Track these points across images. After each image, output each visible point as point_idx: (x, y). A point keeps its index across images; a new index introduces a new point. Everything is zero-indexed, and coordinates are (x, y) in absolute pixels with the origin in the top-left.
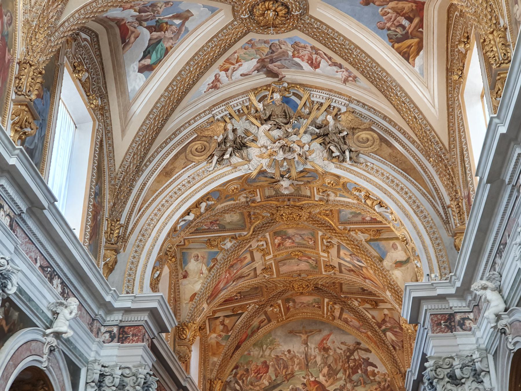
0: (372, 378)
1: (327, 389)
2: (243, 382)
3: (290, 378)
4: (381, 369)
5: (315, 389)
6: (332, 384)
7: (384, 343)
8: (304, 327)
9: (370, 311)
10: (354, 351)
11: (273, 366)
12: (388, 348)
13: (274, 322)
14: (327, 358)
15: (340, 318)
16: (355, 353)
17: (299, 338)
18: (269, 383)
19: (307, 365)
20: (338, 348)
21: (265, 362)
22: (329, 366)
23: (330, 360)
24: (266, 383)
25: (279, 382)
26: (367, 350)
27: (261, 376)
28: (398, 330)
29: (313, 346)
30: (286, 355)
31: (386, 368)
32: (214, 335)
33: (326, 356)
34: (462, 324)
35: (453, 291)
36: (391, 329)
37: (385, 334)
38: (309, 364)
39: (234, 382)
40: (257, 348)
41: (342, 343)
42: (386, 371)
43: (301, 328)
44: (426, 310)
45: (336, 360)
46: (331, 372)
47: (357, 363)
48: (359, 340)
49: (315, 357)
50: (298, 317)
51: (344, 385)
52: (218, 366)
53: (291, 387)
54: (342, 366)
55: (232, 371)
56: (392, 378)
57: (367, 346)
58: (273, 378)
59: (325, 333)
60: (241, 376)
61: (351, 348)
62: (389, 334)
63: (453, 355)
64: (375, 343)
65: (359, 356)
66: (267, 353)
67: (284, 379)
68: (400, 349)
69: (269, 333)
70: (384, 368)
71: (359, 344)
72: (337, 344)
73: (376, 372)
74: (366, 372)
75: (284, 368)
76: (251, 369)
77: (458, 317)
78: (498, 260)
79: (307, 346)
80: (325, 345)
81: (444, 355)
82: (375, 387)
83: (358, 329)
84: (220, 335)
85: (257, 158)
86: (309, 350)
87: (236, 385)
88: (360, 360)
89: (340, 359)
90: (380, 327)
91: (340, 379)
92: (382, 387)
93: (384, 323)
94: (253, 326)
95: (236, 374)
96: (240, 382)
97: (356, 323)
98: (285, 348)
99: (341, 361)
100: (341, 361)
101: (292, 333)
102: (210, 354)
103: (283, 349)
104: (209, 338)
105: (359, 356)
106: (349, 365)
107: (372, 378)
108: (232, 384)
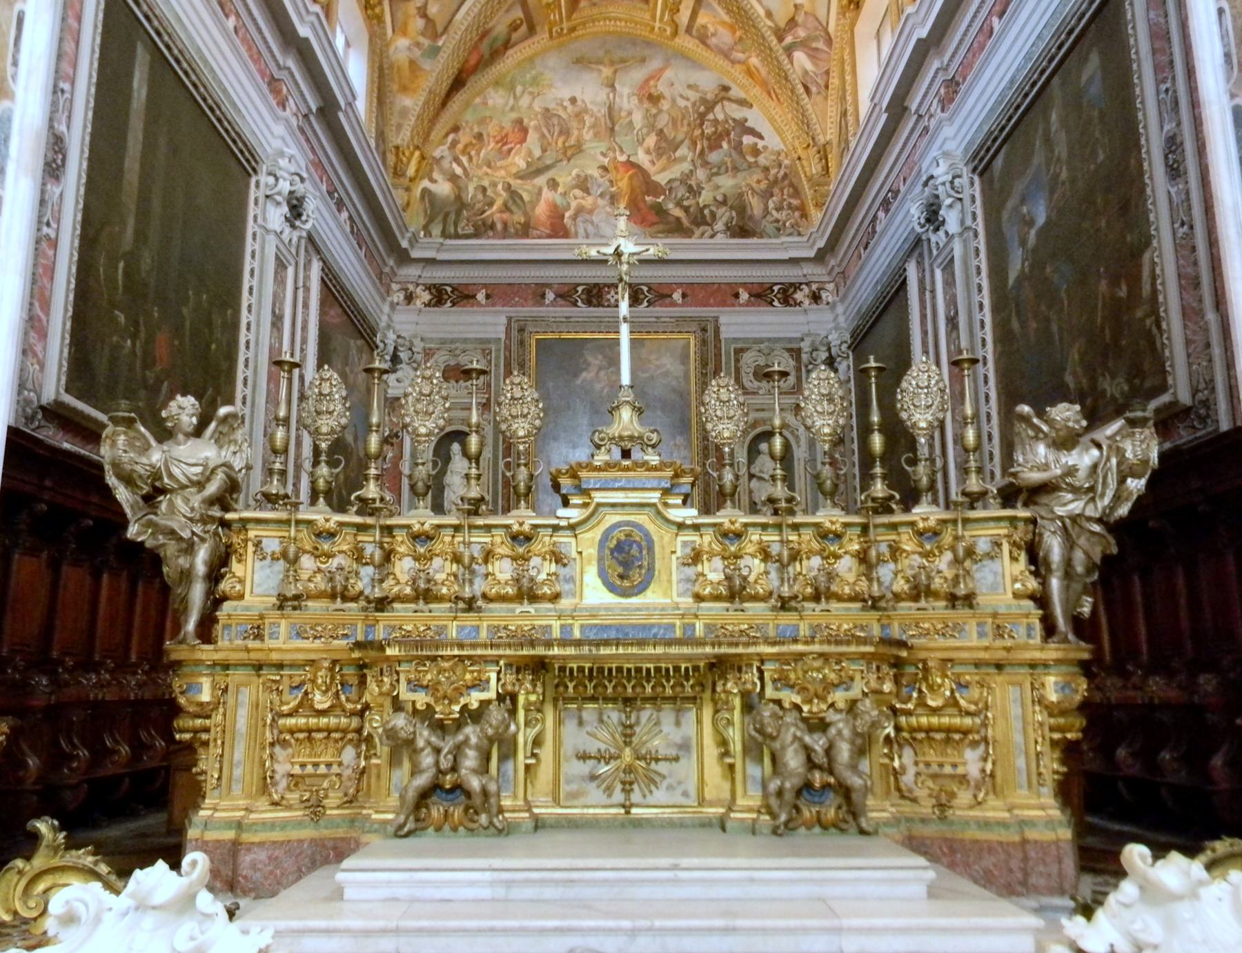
0: (751, 160)
1: (654, 178)
2: (470, 159)
3: (573, 155)
4: (772, 141)
5: (625, 181)
6: (664, 169)
7: (786, 78)
8: (607, 52)
10: (716, 103)
11: (537, 128)
12: (792, 91)
13: (542, 38)
14: (655, 116)
15: (689, 30)
16: (718, 108)
17: (595, 74)
18: (528, 163)
19: (612, 130)
20: (681, 96)
21: (519, 122)
22: (660, 133)
23: (663, 121)
24: (522, 164)
25: (548, 162)
26: (743, 103)
27: (510, 151)
28: (820, 45)
30: (565, 108)
31: (783, 139)
32: (402, 42)
33: (654, 111)
36: (804, 44)
37: (790, 56)
38: (617, 128)
39: (449, 159)
40: (501, 92)
41: (689, 87)
42: (782, 147)
43: (601, 53)
45: (674, 122)
46: (664, 145)
47: (720, 129)
48: (727, 82)
49: (630, 113)
50: (595, 29)
51: (691, 171)
52: (413, 119)
53: (574, 173)
54: (687, 133)
55: (447, 135)
56: (793, 161)
57: (742, 95)
58: (537, 153)
59: (655, 64)
60: (466, 146)
61: (710, 97)
62: (800, 56)
64: (764, 84)
65: (726, 114)
66: (525, 101)
67: (561, 157)
68: (819, 93)
69: (531, 60)
70: (777, 139)
71: (726, 89)
72: (680, 88)
73: (760, 146)
74: (738, 147)
75: (561, 133)
76: (488, 135)
80: (653, 91)
82: (755, 177)
83: (726, 55)
84: (418, 44)
86: (617, 99)
87: (455, 165)
88: (727, 121)
89: (683, 118)
90: (781, 39)
91: (683, 159)
92: (771, 178)
93: (790, 29)
94: (494, 34)
95: (454, 144)
96: (464, 160)
97: (724, 37)
98: (565, 93)
99: (685, 122)
100: (685, 122)
101: (581, 62)
102: (395, 87)
103: (560, 96)
104: (392, 49)
105: (726, 114)
106: (703, 133)
107: (751, 160)
108: (446, 164)
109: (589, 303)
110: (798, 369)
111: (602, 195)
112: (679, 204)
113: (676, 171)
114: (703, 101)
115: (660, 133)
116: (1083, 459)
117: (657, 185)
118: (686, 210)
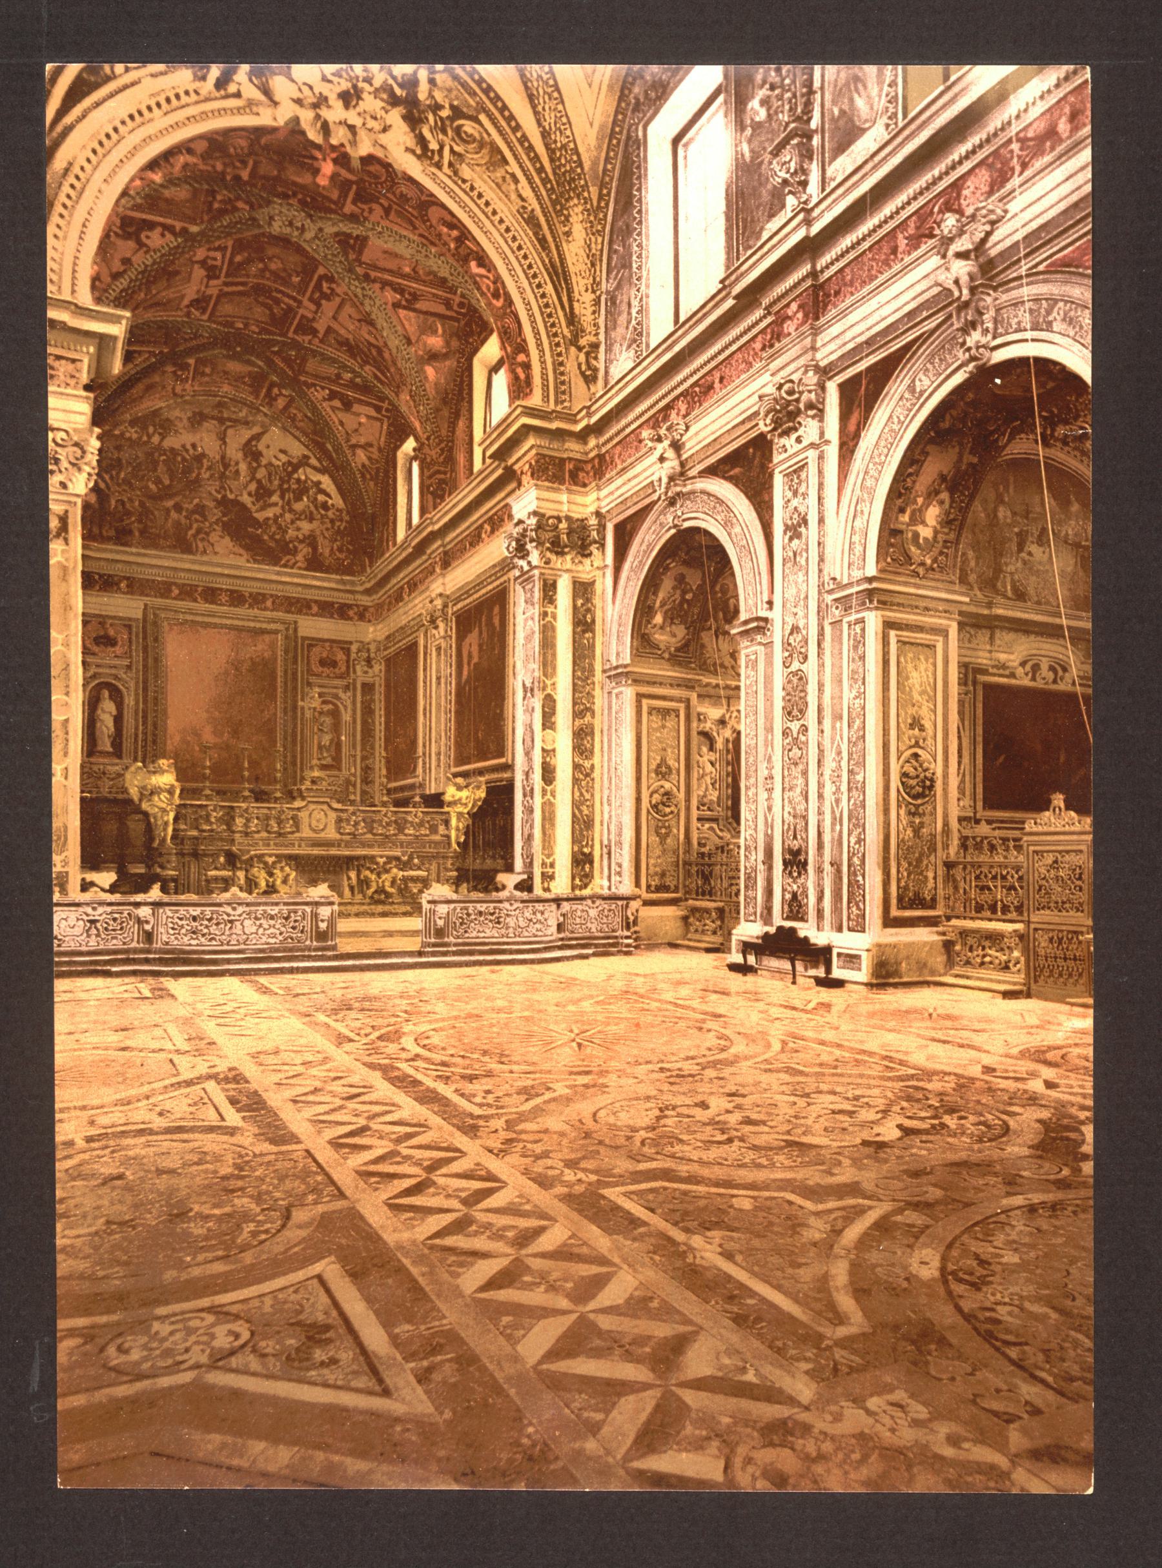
6: (262, 509)
9: (341, 415)
23: (261, 473)
29: (236, 446)
30: (187, 451)
34: (574, 478)
35: (578, 427)
41: (281, 451)
44: (532, 447)
45: (270, 474)
49: (237, 463)
53: (196, 501)
61: (295, 461)
62: (359, 452)
63: (562, 515)
77: (569, 466)
78: (682, 406)
79: (225, 443)
81: (549, 513)
85: (292, 104)
91: (276, 504)
109: (207, 601)
110: (348, 661)
111: (216, 523)
112: (272, 537)
113: (270, 513)
114: (290, 463)
115: (259, 482)
116: (464, 794)
117: (256, 521)
118: (276, 541)
